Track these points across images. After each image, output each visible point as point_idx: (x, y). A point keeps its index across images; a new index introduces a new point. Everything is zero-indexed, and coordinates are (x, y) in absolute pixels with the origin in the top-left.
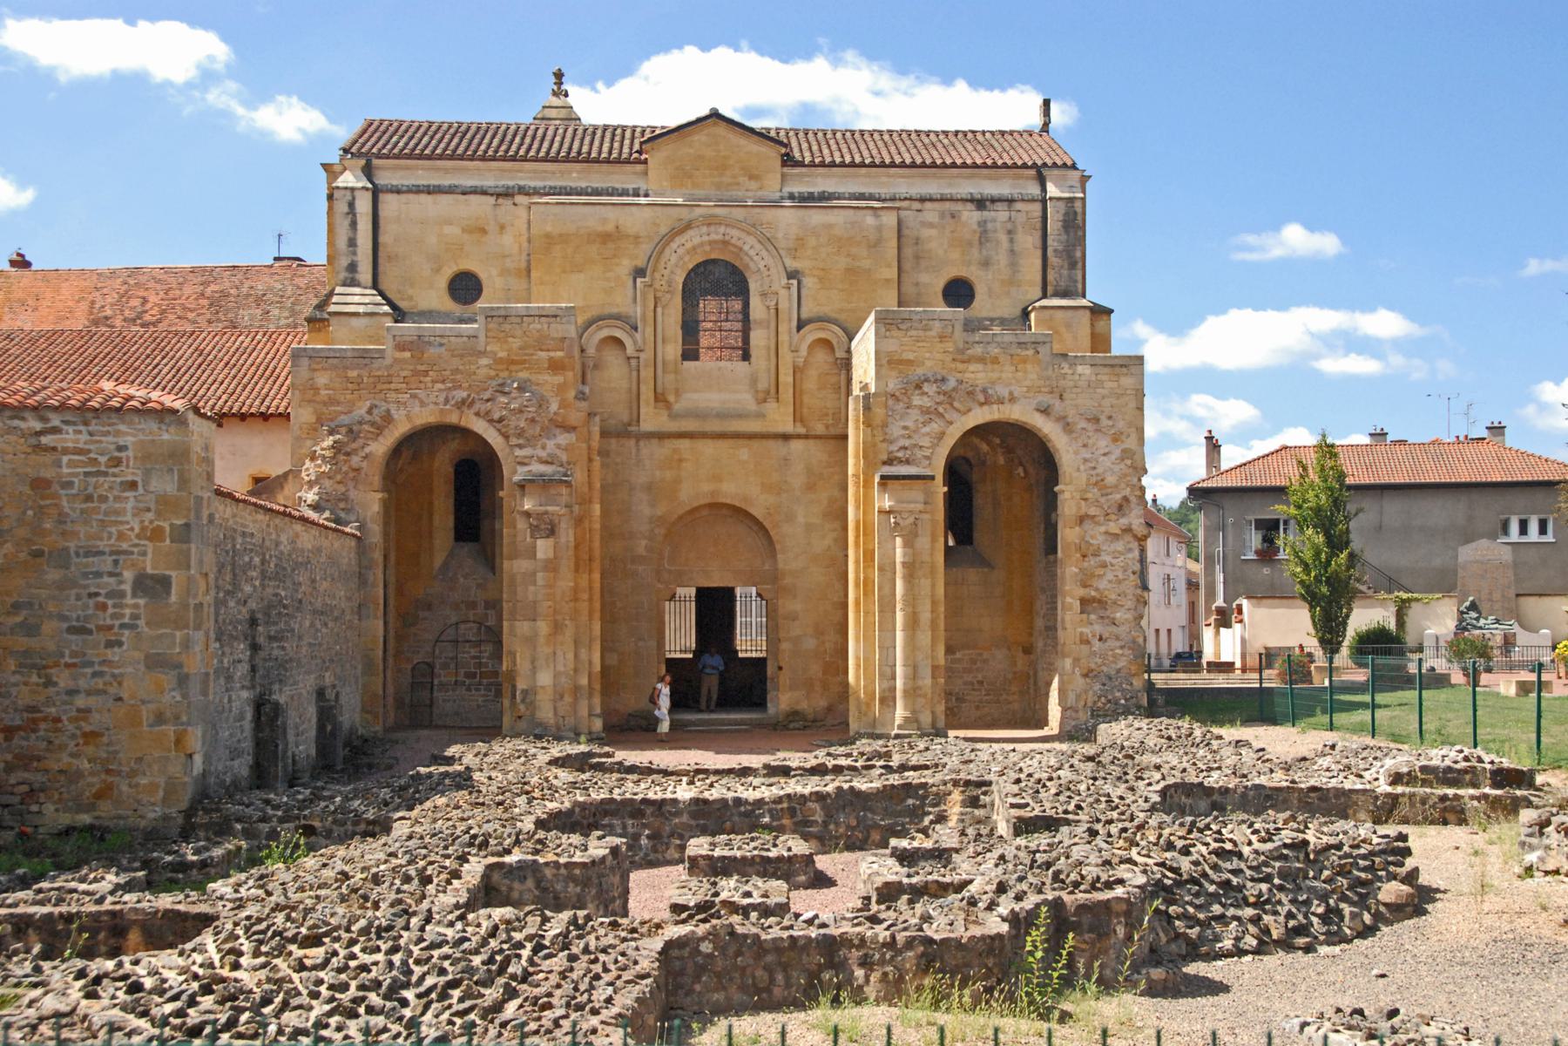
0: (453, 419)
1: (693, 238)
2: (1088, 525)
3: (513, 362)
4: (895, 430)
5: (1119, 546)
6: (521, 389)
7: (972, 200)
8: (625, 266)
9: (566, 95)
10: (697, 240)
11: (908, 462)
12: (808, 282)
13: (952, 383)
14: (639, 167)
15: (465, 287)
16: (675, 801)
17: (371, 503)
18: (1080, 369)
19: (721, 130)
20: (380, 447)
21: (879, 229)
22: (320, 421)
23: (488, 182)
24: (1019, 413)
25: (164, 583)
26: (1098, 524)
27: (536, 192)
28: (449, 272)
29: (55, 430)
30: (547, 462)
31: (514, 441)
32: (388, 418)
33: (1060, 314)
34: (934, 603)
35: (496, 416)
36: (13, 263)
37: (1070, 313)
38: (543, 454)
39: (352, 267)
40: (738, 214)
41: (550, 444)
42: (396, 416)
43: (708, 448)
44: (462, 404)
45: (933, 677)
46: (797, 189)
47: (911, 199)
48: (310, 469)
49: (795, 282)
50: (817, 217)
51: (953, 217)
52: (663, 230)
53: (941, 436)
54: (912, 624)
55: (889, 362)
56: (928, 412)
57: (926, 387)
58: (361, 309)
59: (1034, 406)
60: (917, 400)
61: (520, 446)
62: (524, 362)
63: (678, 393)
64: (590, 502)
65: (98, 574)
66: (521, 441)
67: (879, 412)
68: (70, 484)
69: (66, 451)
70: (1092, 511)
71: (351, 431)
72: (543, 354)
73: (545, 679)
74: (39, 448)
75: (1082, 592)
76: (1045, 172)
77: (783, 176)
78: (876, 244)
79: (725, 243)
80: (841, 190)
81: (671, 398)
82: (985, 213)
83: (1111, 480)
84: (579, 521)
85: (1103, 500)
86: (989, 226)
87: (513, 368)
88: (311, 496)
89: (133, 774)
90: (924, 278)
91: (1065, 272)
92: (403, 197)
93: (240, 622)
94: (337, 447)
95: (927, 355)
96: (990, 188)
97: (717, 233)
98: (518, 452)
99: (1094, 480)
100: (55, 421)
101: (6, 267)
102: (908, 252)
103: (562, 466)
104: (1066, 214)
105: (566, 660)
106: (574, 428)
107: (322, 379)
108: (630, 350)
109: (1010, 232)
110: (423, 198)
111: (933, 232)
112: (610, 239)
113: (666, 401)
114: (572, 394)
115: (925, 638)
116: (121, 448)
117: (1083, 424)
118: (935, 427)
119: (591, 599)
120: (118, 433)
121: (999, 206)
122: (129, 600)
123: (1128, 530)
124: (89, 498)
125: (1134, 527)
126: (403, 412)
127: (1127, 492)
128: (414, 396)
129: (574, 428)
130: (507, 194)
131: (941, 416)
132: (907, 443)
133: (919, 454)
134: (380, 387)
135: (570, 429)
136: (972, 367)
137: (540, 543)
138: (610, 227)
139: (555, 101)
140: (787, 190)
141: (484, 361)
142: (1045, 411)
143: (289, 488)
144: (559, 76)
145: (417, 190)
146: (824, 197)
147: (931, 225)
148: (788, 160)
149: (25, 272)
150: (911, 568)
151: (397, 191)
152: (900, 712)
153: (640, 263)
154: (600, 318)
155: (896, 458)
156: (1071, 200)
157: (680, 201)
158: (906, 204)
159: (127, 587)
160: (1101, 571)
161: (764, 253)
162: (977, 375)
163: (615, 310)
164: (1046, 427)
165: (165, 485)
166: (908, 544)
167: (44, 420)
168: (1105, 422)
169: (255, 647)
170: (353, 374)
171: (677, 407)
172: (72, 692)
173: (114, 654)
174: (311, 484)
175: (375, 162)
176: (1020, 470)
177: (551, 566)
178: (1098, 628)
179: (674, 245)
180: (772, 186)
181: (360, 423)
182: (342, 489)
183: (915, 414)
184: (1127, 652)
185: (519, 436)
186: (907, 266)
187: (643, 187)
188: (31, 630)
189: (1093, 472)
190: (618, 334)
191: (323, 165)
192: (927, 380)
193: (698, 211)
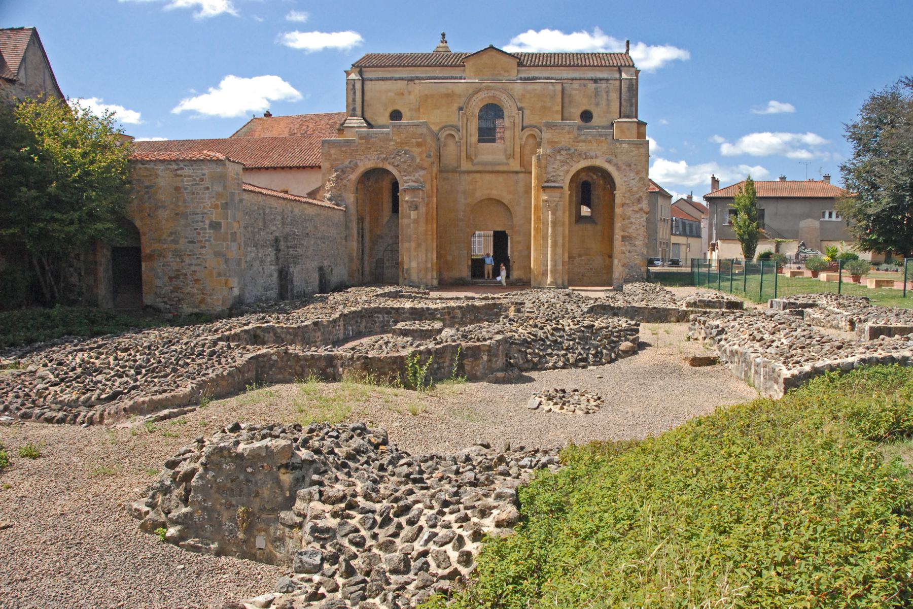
0: (380, 165)
1: (482, 95)
2: (625, 207)
3: (403, 143)
4: (550, 169)
5: (638, 215)
6: (405, 154)
7: (592, 80)
8: (455, 106)
9: (446, 42)
10: (483, 96)
11: (555, 181)
12: (527, 112)
13: (572, 150)
14: (463, 68)
15: (396, 115)
16: (403, 308)
17: (350, 198)
18: (624, 145)
19: (494, 53)
20: (354, 176)
21: (554, 91)
22: (332, 167)
23: (404, 75)
25: (219, 224)
27: (423, 79)
28: (390, 110)
29: (182, 169)
30: (415, 182)
31: (403, 174)
32: (356, 165)
33: (625, 124)
34: (564, 237)
35: (396, 164)
36: (265, 115)
37: (629, 124)
38: (414, 179)
39: (354, 109)
40: (499, 85)
41: (417, 175)
43: (487, 177)
44: (385, 159)
45: (563, 265)
46: (523, 75)
47: (568, 79)
48: (328, 185)
50: (530, 87)
51: (584, 86)
52: (470, 92)
53: (568, 172)
54: (555, 245)
57: (562, 152)
58: (356, 125)
60: (558, 157)
61: (405, 176)
63: (476, 156)
64: (432, 197)
65: (197, 222)
67: (543, 162)
68: (186, 189)
69: (185, 176)
70: (627, 202)
71: (343, 170)
72: (414, 140)
73: (414, 264)
74: (177, 175)
75: (622, 233)
76: (622, 69)
77: (518, 71)
78: (553, 97)
79: (494, 97)
80: (540, 75)
81: (473, 158)
82: (598, 85)
83: (635, 189)
84: (427, 204)
88: (328, 195)
89: (211, 295)
90: (573, 110)
91: (628, 108)
92: (373, 82)
93: (269, 240)
94: (338, 177)
96: (599, 75)
98: (404, 178)
100: (182, 165)
101: (263, 116)
102: (567, 100)
104: (629, 85)
105: (422, 257)
107: (332, 151)
108: (457, 139)
109: (607, 92)
110: (381, 82)
111: (577, 92)
112: (450, 96)
113: (471, 159)
114: (425, 155)
115: (559, 250)
116: (204, 175)
117: (624, 167)
118: (565, 168)
119: (432, 235)
120: (202, 169)
121: (602, 82)
122: (208, 231)
123: (641, 209)
124: (193, 194)
127: (641, 194)
128: (366, 157)
130: (411, 80)
131: (568, 163)
132: (554, 174)
133: (559, 178)
135: (424, 169)
136: (580, 144)
137: (412, 212)
138: (450, 91)
139: (442, 45)
140: (519, 76)
141: (392, 143)
142: (609, 162)
143: (321, 192)
144: (443, 35)
145: (378, 79)
146: (534, 78)
147: (576, 89)
148: (520, 64)
149: (269, 118)
150: (554, 224)
151: (371, 80)
152: (549, 279)
153: (461, 105)
156: (631, 79)
157: (477, 81)
158: (566, 81)
159: (207, 226)
160: (630, 225)
161: (509, 101)
162: (582, 147)
163: (451, 123)
164: (610, 169)
165: (218, 188)
166: (553, 214)
167: (178, 165)
168: (633, 166)
169: (278, 250)
170: (344, 149)
171: (476, 161)
172: (191, 265)
173: (204, 251)
174: (328, 191)
175: (363, 69)
176: (609, 186)
177: (416, 221)
178: (628, 248)
179: (474, 98)
180: (513, 74)
181: (346, 167)
182: (339, 192)
183: (558, 163)
184: (640, 257)
185: (405, 172)
186: (566, 105)
187: (464, 76)
188: (175, 242)
190: (453, 133)
191: (345, 71)
193: (484, 84)
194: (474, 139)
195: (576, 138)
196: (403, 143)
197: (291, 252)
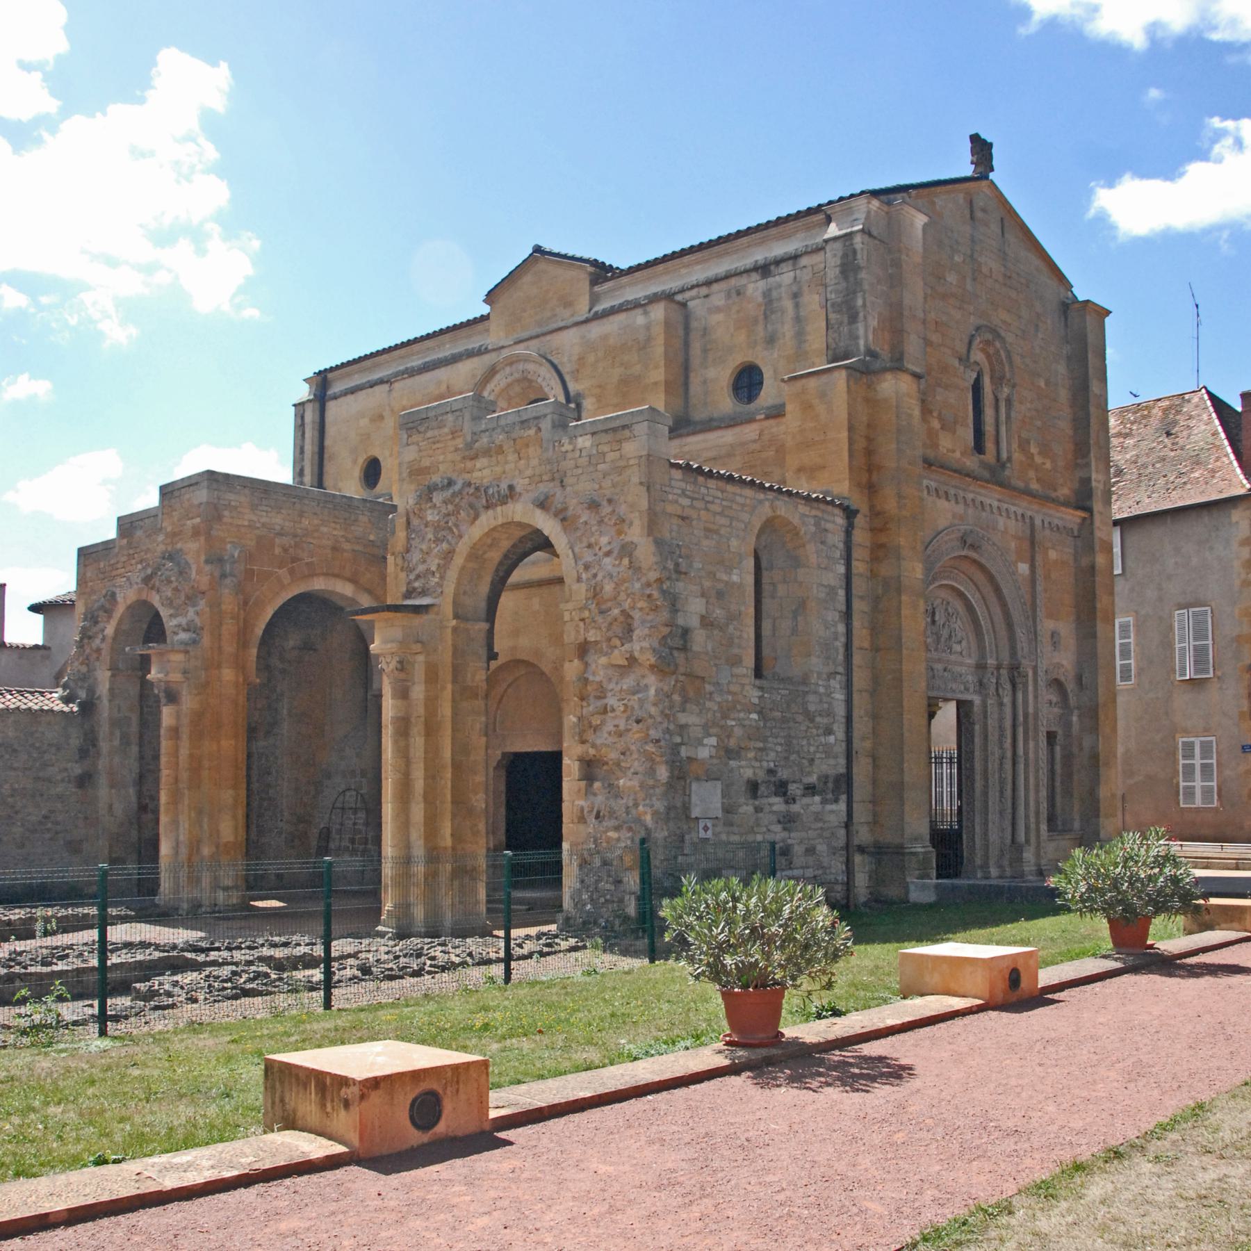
10: (503, 384)
21: (648, 327)
47: (698, 286)
53: (449, 555)
78: (644, 346)
82: (771, 280)
86: (775, 294)
90: (711, 373)
102: (696, 347)
104: (845, 256)
111: (720, 317)
121: (785, 267)
147: (718, 310)
158: (694, 292)
162: (483, 471)
177: (175, 732)
186: (695, 361)
195: (469, 446)
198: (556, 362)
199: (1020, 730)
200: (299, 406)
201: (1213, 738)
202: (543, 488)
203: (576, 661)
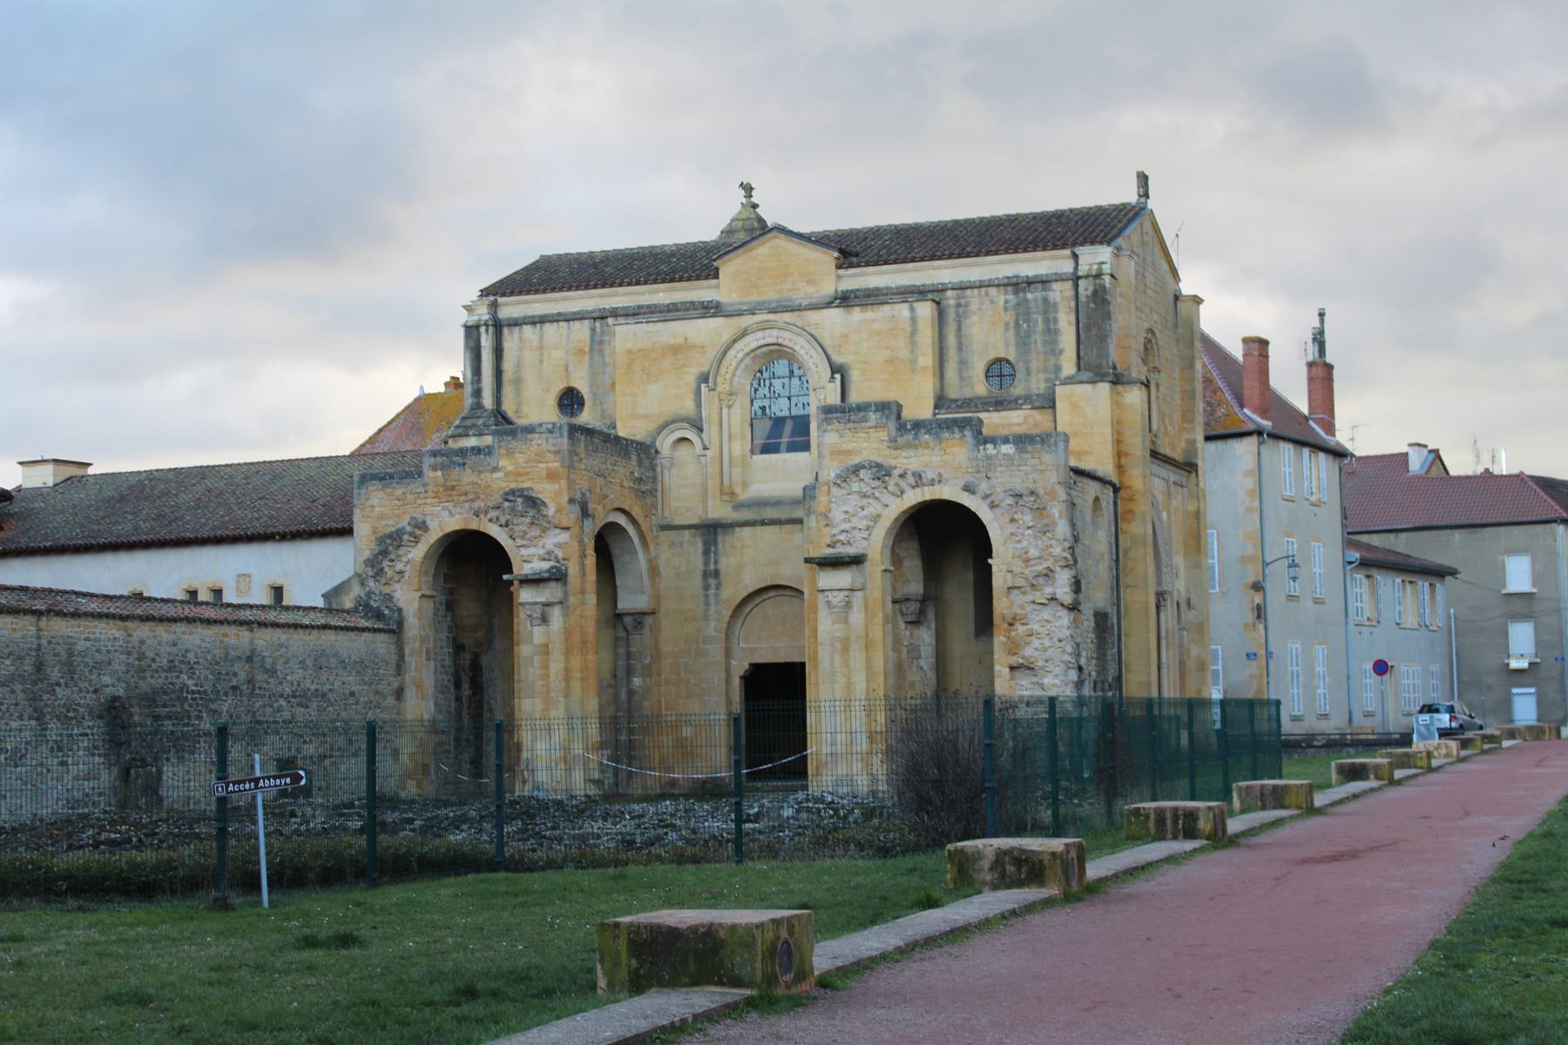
3: (520, 475)
10: (754, 345)
20: (417, 553)
24: (949, 492)
26: (1024, 593)
30: (544, 559)
31: (520, 542)
32: (423, 526)
35: (503, 520)
42: (431, 527)
49: (838, 376)
53: (876, 518)
55: (831, 454)
56: (865, 496)
59: (962, 483)
60: (856, 486)
62: (528, 474)
63: (745, 485)
66: (524, 542)
73: (541, 747)
77: (839, 277)
85: (1027, 572)
87: (519, 479)
95: (865, 445)
97: (771, 336)
98: (523, 551)
99: (1018, 553)
103: (558, 562)
106: (568, 528)
114: (565, 498)
125: (1058, 596)
126: (436, 522)
129: (568, 528)
132: (846, 526)
134: (419, 502)
137: (535, 629)
138: (680, 340)
142: (968, 489)
153: (705, 369)
154: (673, 422)
155: (838, 541)
161: (812, 352)
177: (545, 650)
185: (523, 537)
189: (1018, 546)
191: (464, 307)
192: (864, 467)
194: (739, 446)
196: (520, 475)
197: (168, 726)
198: (816, 334)
199: (1163, 643)
200: (472, 331)
201: (1219, 647)
202: (969, 478)
203: (1005, 599)
